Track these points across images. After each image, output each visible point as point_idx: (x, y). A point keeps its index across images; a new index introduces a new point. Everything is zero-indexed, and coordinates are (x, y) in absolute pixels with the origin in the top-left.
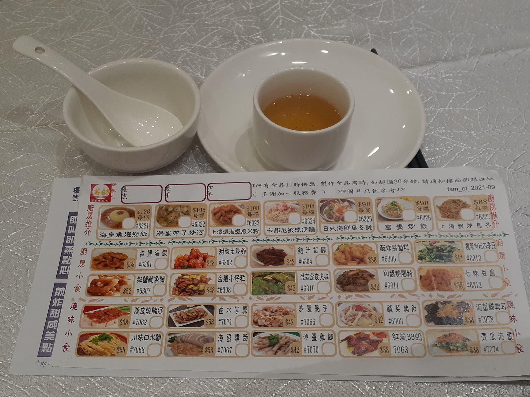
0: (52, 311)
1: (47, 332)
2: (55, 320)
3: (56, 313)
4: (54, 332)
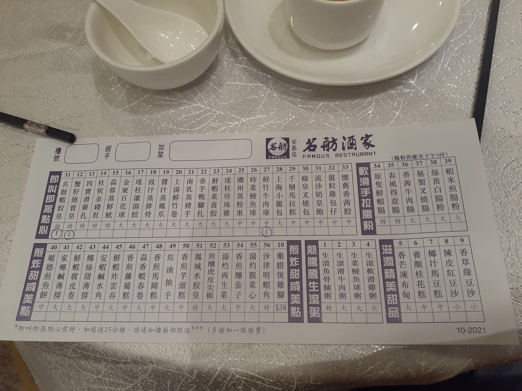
0: (31, 273)
1: (25, 295)
2: (34, 283)
3: (35, 275)
4: (32, 295)
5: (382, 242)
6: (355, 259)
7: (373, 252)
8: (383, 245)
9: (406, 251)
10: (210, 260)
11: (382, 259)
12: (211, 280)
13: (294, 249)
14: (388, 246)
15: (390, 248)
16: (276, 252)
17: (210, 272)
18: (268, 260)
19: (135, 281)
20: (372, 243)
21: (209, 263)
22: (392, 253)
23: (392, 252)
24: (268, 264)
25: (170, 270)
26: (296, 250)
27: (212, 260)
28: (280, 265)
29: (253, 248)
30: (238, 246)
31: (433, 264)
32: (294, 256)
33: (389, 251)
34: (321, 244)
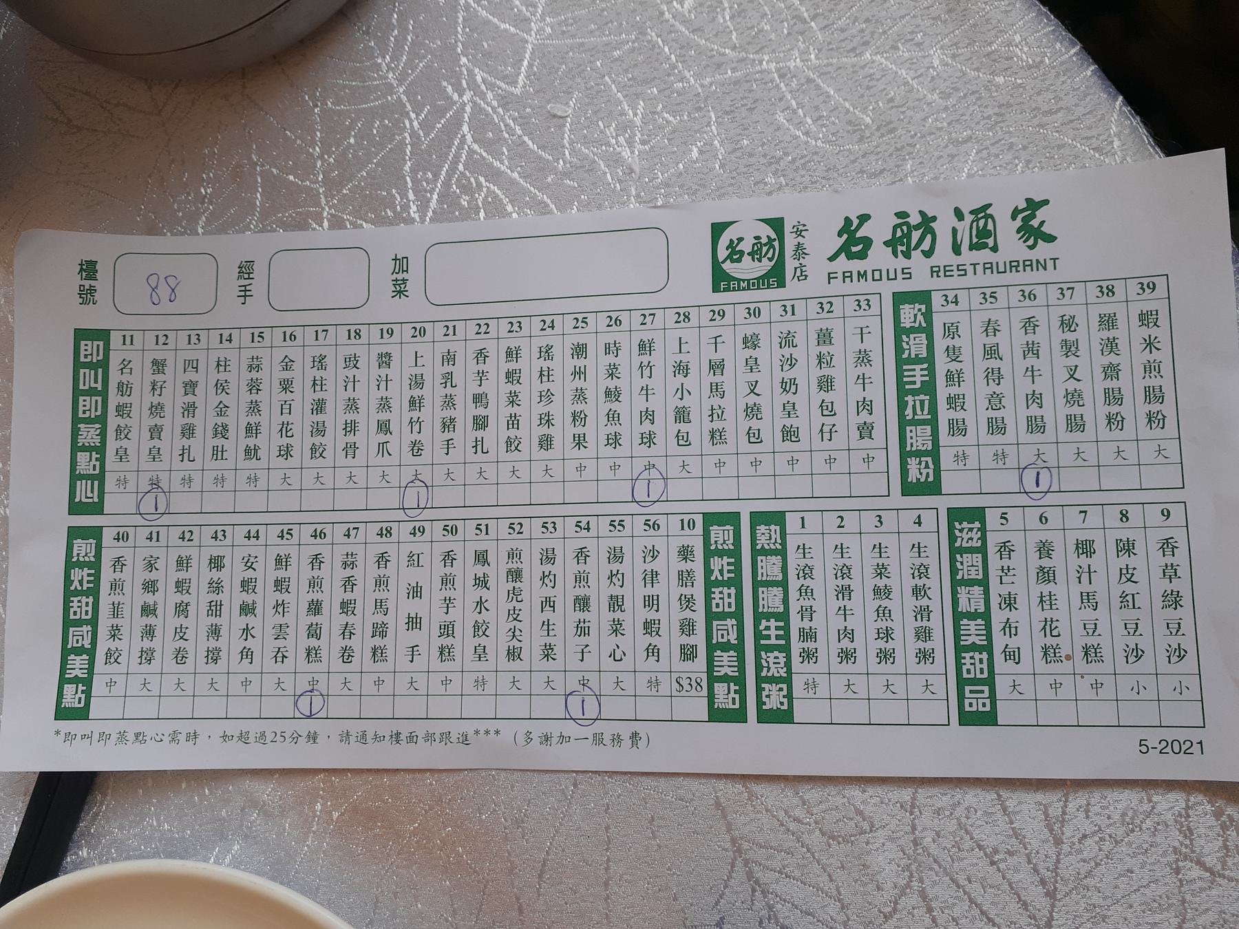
5: (955, 515)
6: (880, 561)
7: (929, 541)
8: (957, 524)
9: (1017, 540)
10: (510, 565)
11: (952, 560)
12: (514, 615)
13: (721, 535)
14: (971, 526)
15: (975, 530)
16: (676, 543)
17: (511, 595)
18: (655, 566)
19: (332, 620)
20: (929, 519)
21: (509, 572)
22: (979, 544)
23: (980, 541)
24: (655, 574)
25: (416, 592)
26: (726, 538)
27: (515, 566)
28: (685, 578)
29: (616, 533)
30: (578, 529)
31: (1085, 577)
32: (721, 553)
33: (972, 539)
34: (792, 522)
